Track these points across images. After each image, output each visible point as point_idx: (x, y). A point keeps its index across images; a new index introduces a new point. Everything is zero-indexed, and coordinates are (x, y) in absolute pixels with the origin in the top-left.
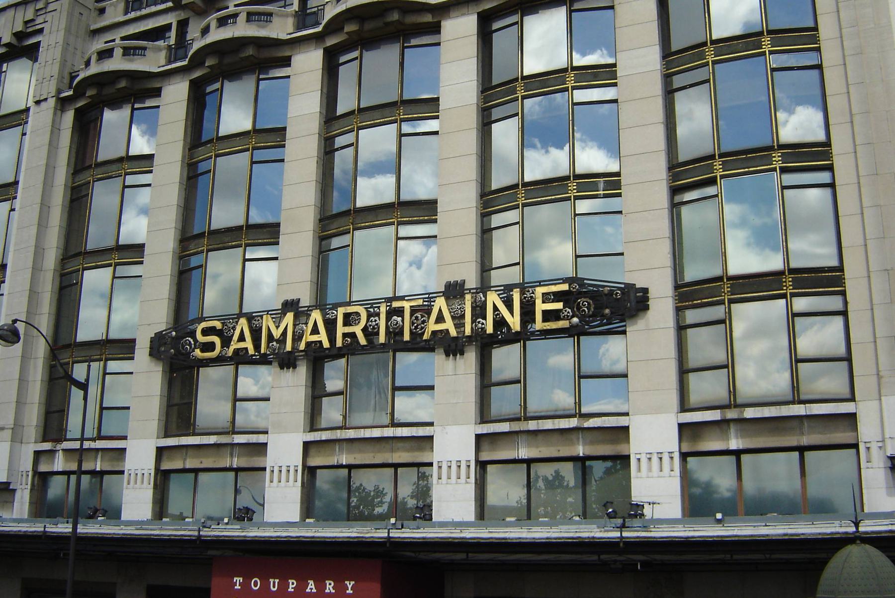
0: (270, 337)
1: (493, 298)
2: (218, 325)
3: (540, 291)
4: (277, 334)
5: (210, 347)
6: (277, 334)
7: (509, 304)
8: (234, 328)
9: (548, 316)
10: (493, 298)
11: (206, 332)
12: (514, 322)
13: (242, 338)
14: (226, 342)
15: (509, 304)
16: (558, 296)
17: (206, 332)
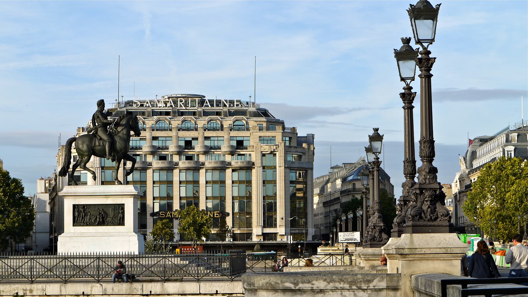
0: (174, 215)
1: (209, 212)
2: (164, 212)
3: (215, 212)
4: (175, 215)
5: (163, 216)
6: (175, 215)
7: (211, 214)
8: (167, 213)
9: (216, 215)
10: (209, 212)
11: (162, 213)
12: (212, 216)
13: (168, 215)
14: (166, 215)
15: (211, 214)
16: (217, 213)
17: (162, 213)
